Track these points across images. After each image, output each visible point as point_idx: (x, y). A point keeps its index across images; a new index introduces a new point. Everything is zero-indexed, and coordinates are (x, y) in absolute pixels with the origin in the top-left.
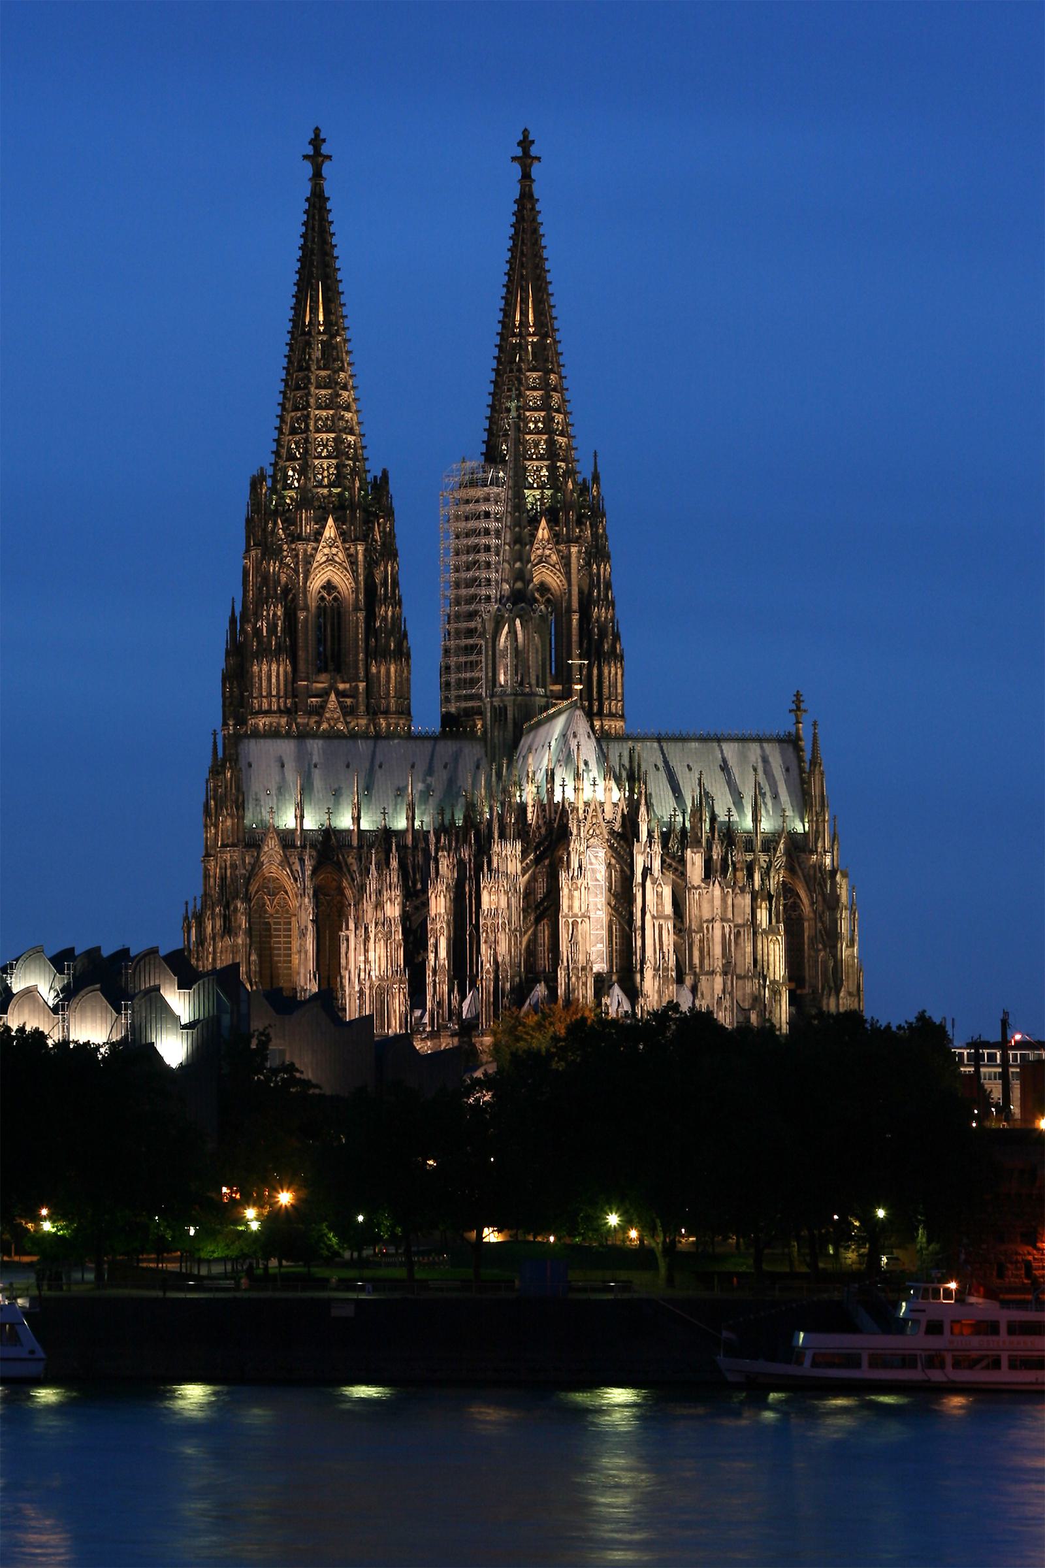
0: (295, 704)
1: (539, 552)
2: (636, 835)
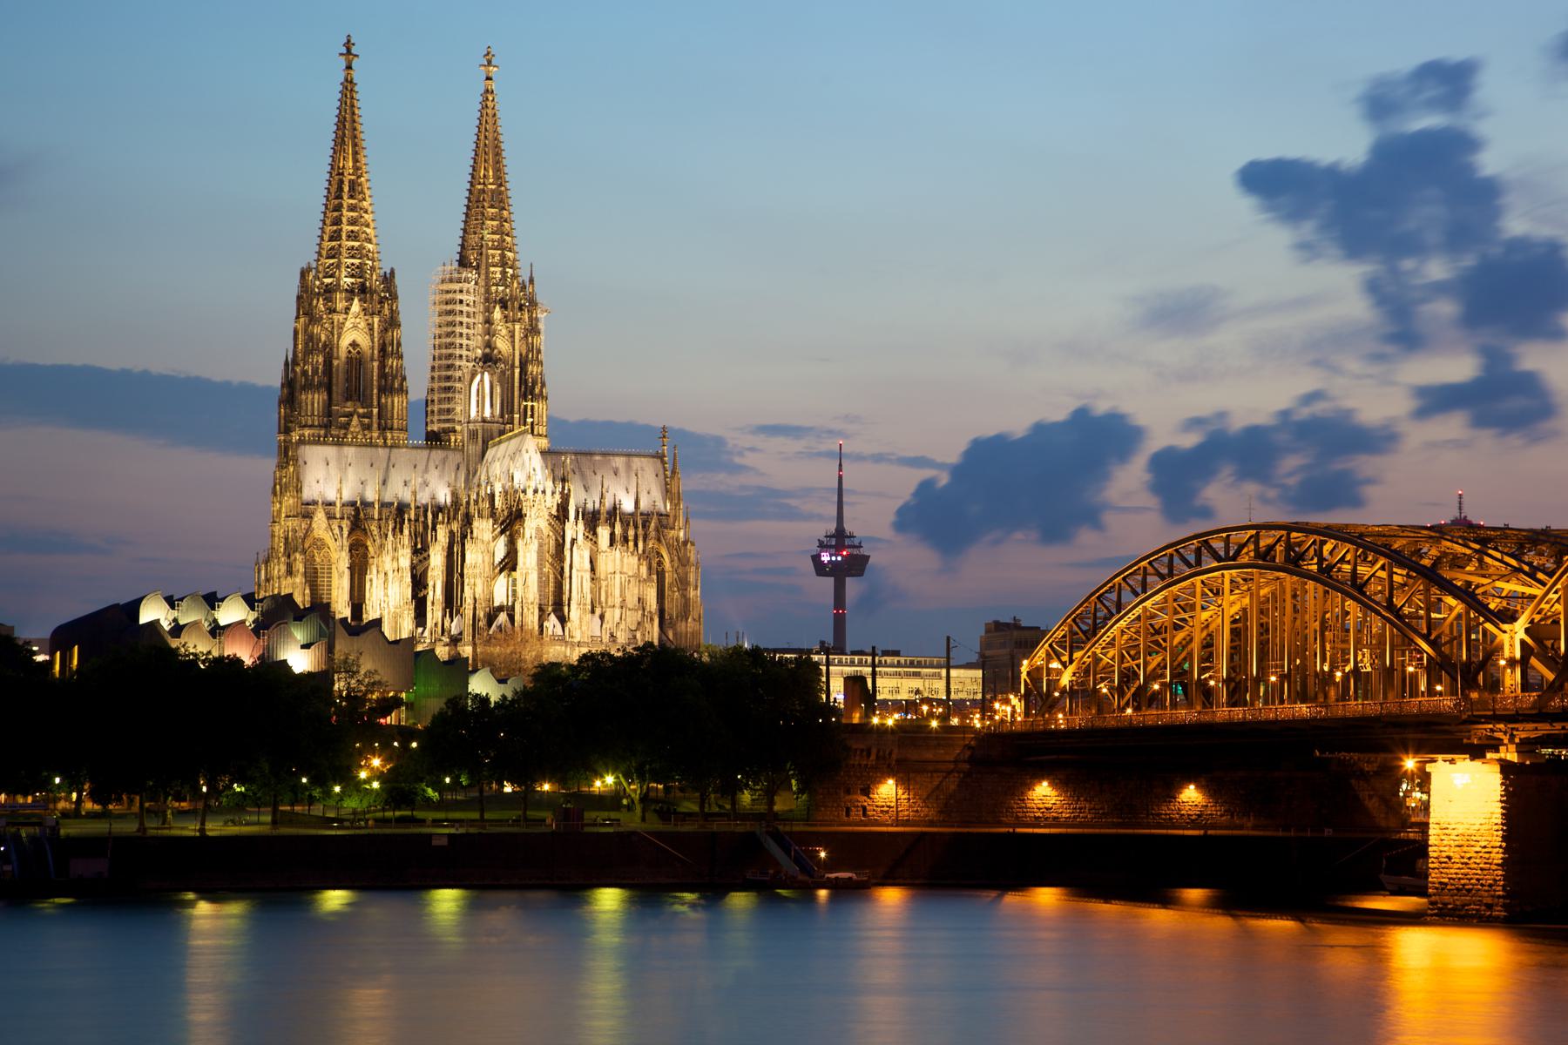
2: (566, 517)
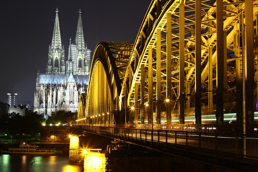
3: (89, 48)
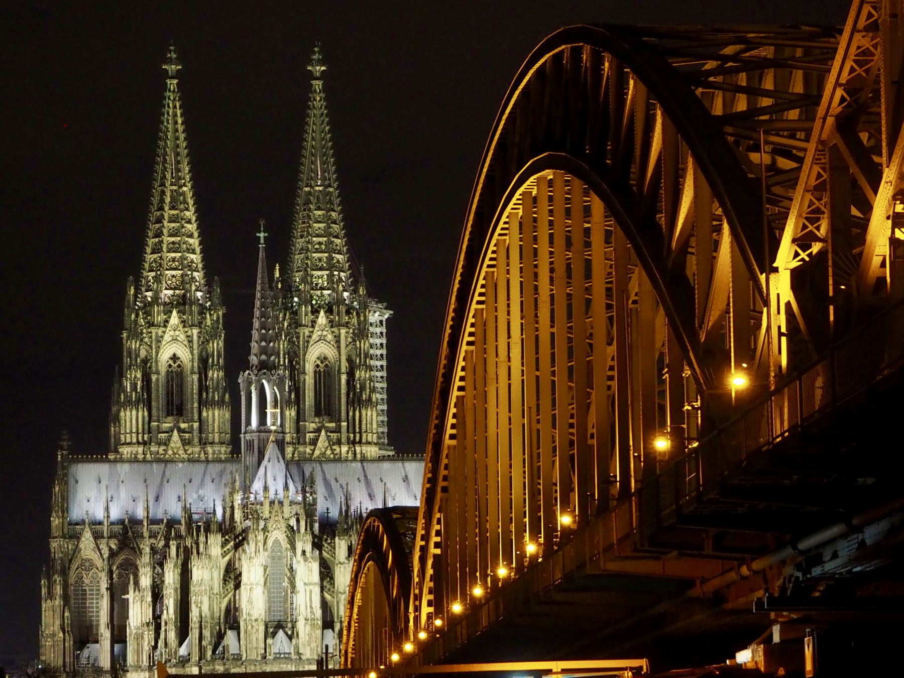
0: (150, 439)
1: (319, 333)
3: (378, 293)
